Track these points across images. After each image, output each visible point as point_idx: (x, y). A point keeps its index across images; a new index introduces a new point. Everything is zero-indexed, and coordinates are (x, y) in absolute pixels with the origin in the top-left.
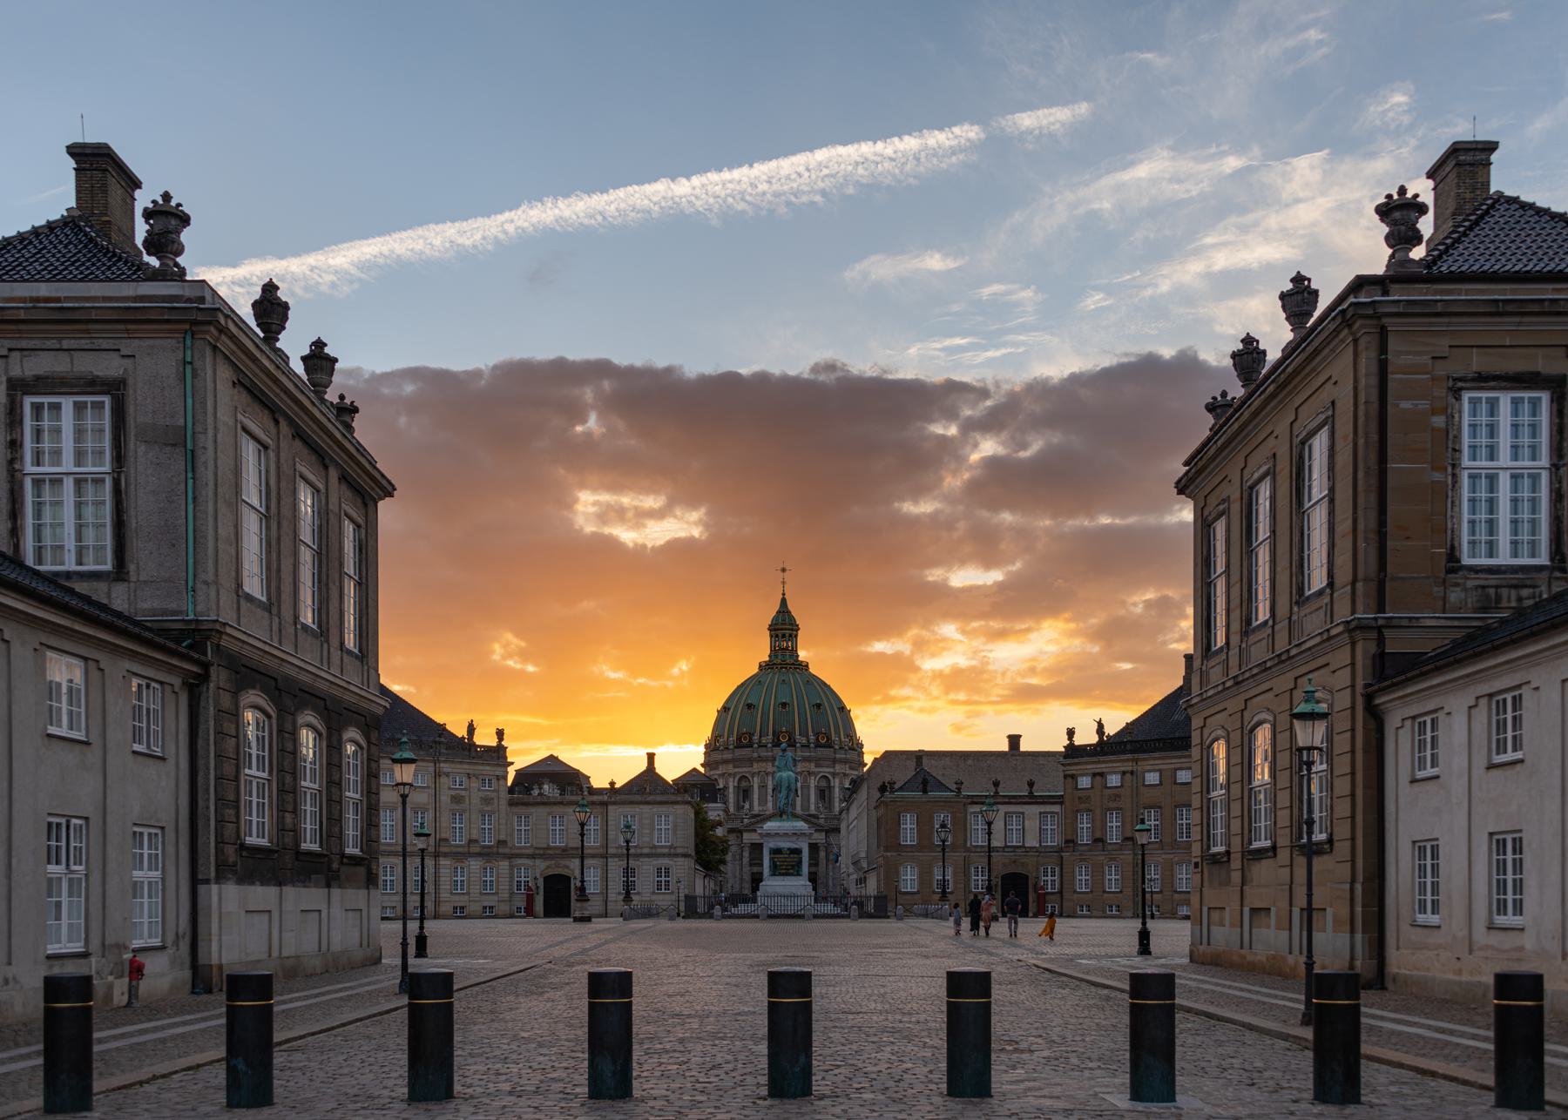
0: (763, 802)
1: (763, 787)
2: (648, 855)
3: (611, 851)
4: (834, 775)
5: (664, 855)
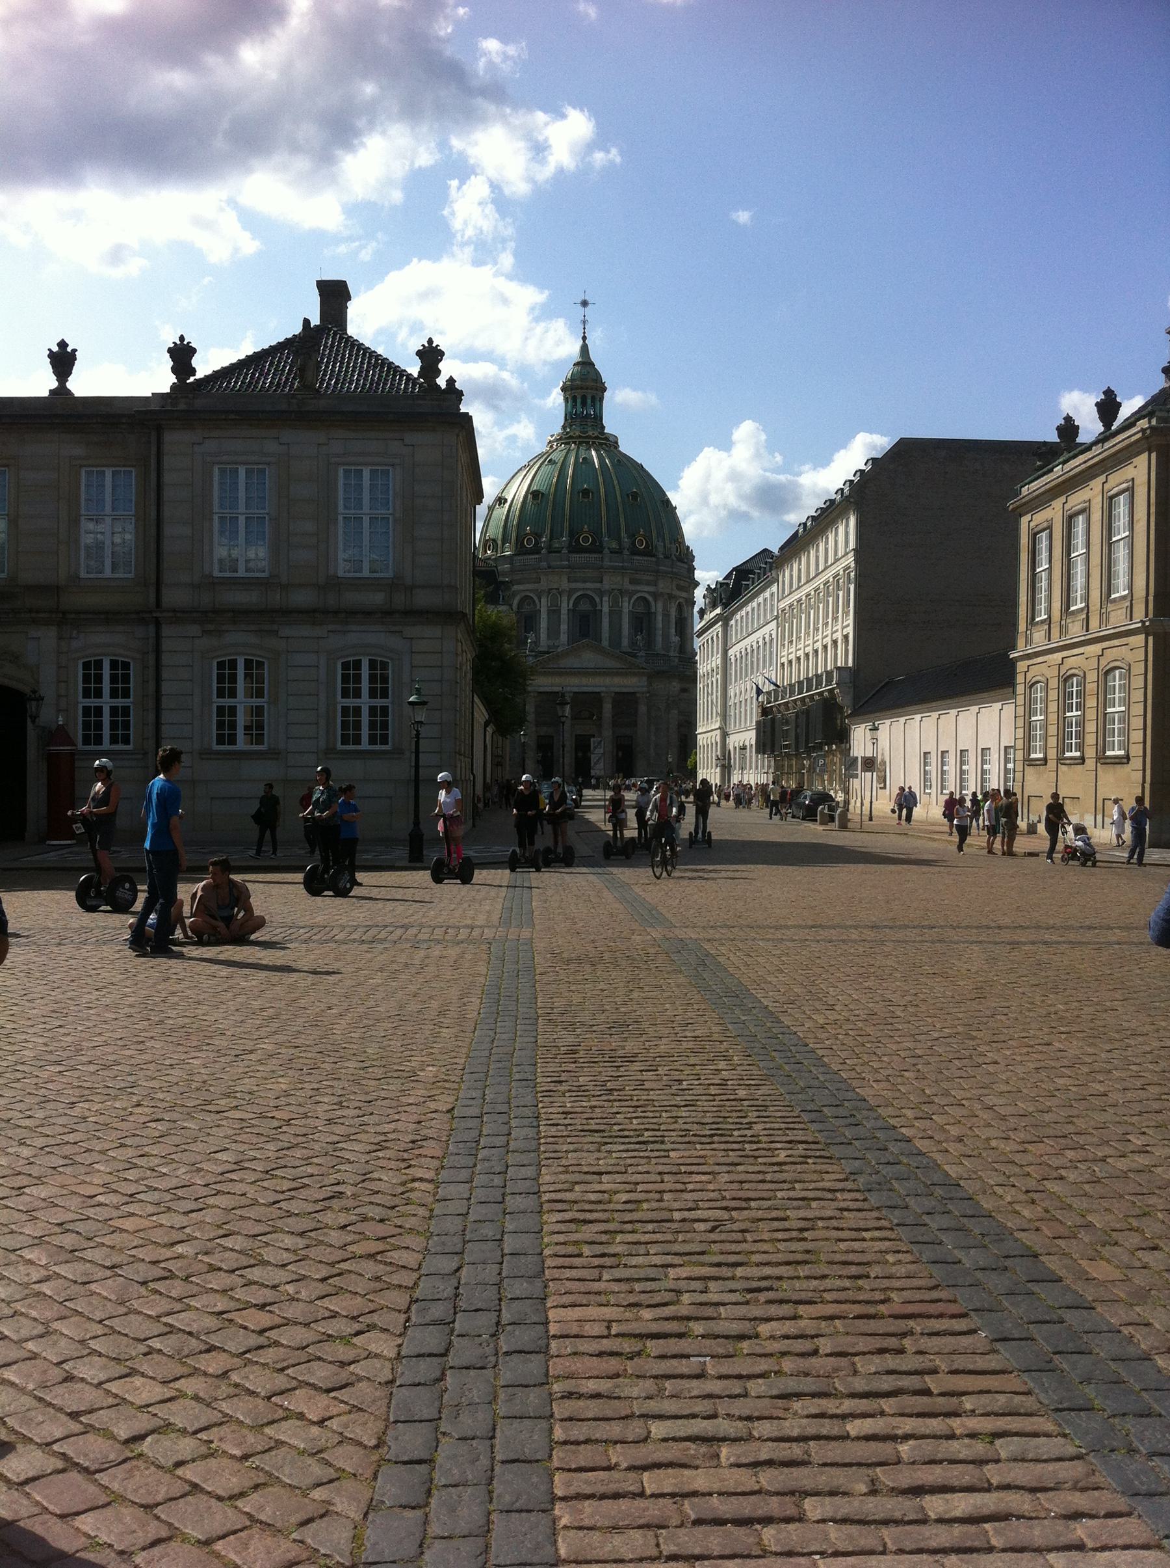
0: (553, 632)
1: (554, 612)
2: (312, 615)
3: (174, 597)
4: (655, 596)
5: (366, 615)
